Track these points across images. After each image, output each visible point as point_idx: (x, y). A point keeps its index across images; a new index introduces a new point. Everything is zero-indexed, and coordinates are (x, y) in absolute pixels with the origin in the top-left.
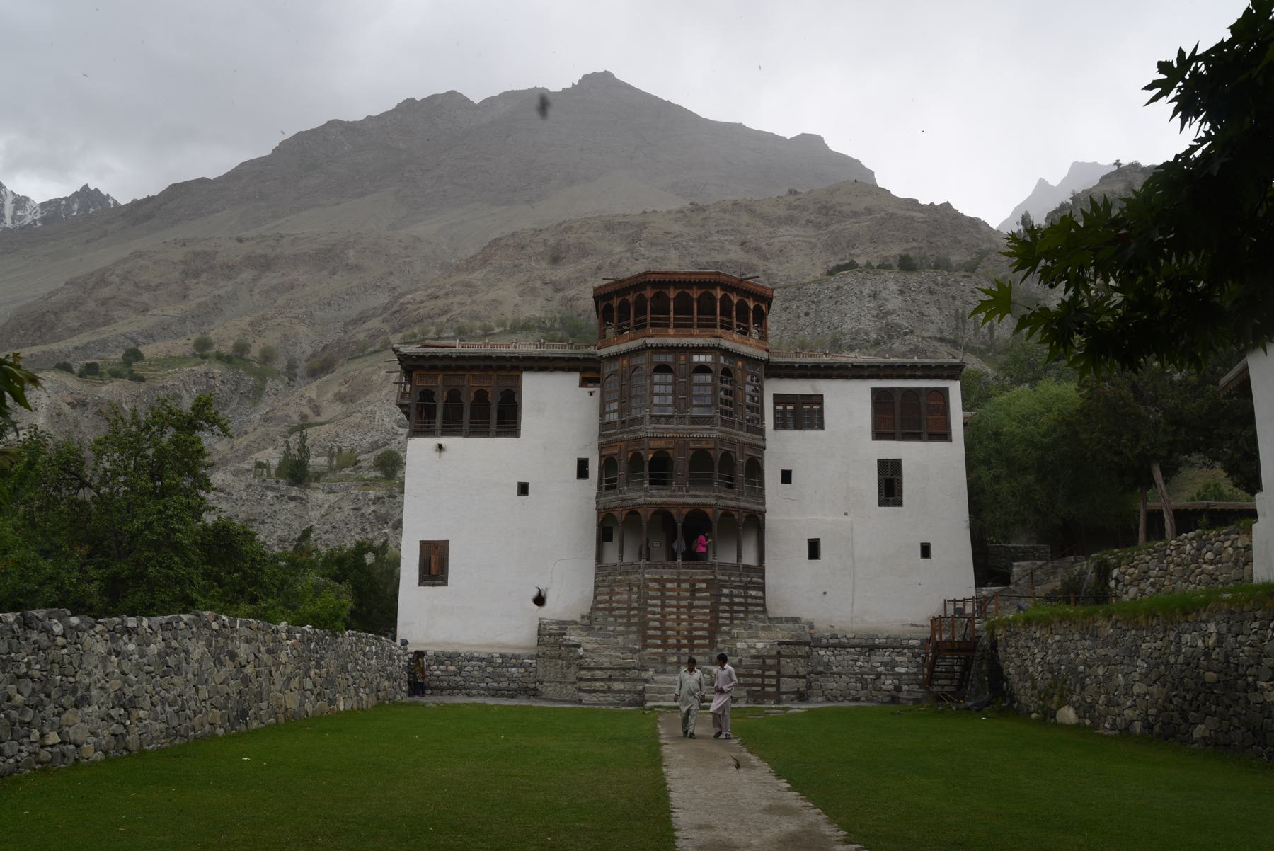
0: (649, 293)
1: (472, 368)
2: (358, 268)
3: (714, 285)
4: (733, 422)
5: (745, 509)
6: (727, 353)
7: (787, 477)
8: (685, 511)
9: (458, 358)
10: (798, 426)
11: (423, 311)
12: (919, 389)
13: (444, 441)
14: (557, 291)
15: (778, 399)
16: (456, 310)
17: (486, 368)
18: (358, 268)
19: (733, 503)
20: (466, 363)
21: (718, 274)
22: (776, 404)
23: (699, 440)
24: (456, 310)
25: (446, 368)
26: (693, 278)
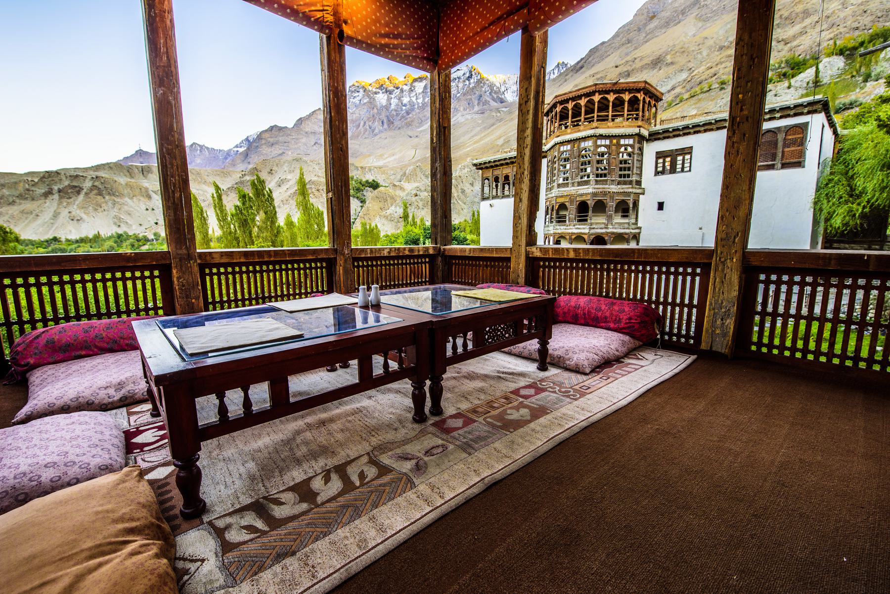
0: (559, 109)
1: (502, 165)
2: (672, 63)
3: (593, 93)
4: (606, 181)
5: (613, 233)
6: (601, 137)
7: (661, 206)
8: (573, 237)
9: (495, 161)
10: (673, 170)
11: (703, 78)
12: (779, 128)
13: (494, 202)
14: (786, 44)
15: (660, 155)
16: (721, 72)
17: (507, 164)
18: (672, 63)
19: (604, 231)
20: (498, 163)
21: (596, 85)
22: (657, 158)
23: (582, 195)
24: (721, 72)
25: (492, 167)
26: (579, 93)
